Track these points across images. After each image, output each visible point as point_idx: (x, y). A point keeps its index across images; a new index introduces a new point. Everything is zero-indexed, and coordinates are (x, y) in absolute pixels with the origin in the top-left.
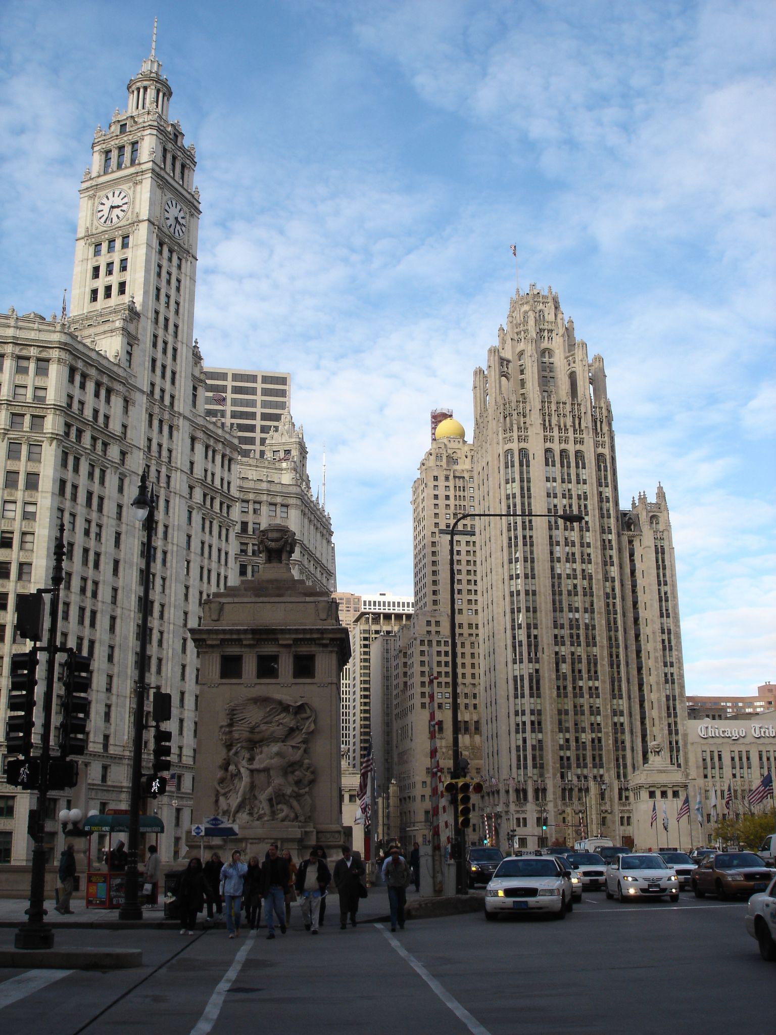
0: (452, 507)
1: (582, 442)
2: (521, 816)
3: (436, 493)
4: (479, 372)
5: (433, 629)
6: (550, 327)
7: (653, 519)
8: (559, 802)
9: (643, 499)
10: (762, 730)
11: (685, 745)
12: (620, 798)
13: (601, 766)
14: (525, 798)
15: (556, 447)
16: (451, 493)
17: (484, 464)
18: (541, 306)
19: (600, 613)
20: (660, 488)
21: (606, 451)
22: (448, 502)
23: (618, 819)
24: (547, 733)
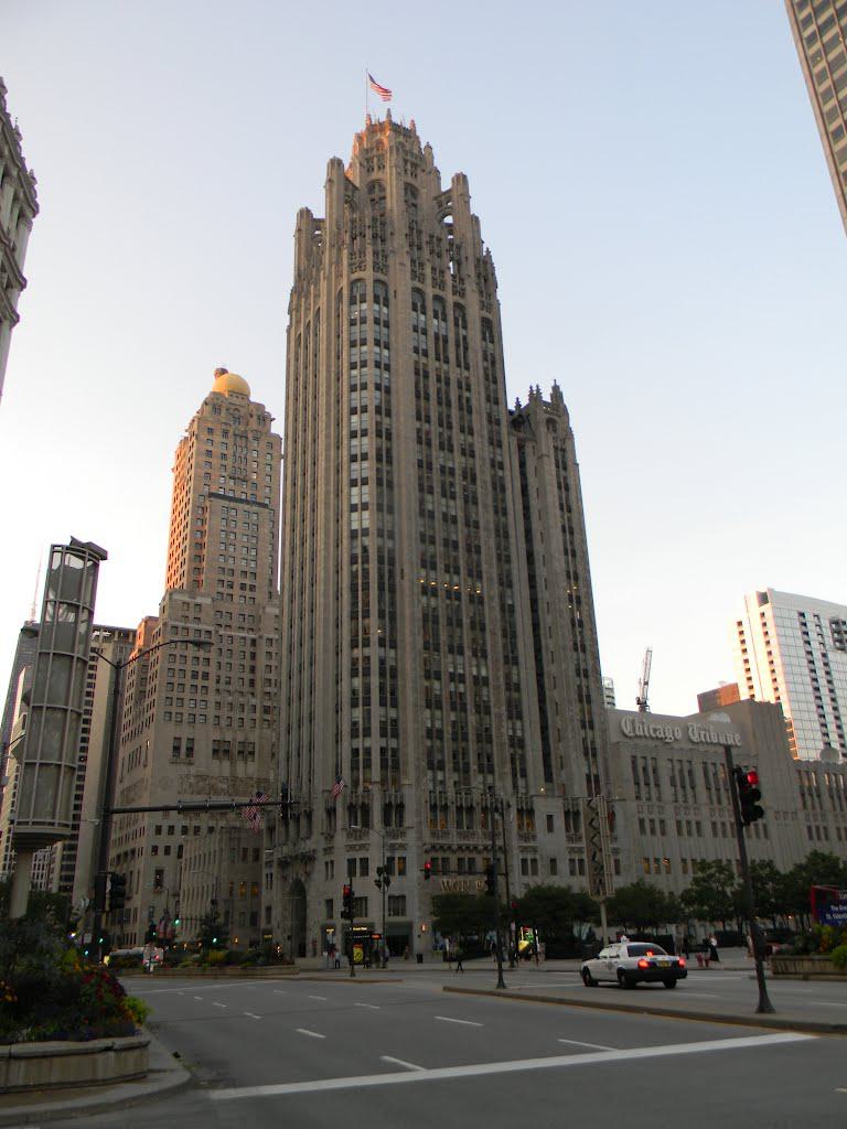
0: (229, 469)
1: (462, 294)
2: (358, 855)
3: (210, 448)
4: (305, 214)
5: (191, 614)
7: (551, 423)
8: (426, 832)
9: (535, 396)
10: (702, 733)
11: (605, 743)
12: (520, 827)
14: (367, 824)
16: (230, 453)
17: (311, 317)
19: (487, 529)
20: (556, 389)
22: (224, 462)
23: (516, 864)
24: (405, 708)
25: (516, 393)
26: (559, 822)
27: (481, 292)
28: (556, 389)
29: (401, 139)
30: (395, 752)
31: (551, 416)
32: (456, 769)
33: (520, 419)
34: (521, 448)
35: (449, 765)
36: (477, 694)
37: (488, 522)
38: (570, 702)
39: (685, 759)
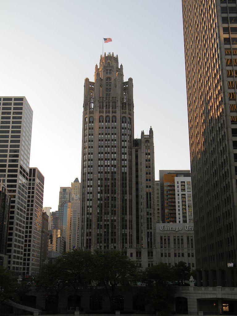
1: (115, 112)
6: (110, 68)
11: (155, 233)
13: (115, 242)
15: (104, 115)
18: (109, 61)
20: (151, 129)
21: (127, 115)
25: (137, 136)
26: (134, 255)
27: (123, 109)
28: (151, 129)
29: (109, 61)
30: (90, 240)
31: (148, 139)
32: (105, 243)
33: (137, 143)
34: (137, 151)
35: (103, 242)
36: (112, 224)
37: (118, 178)
38: (144, 223)
39: (180, 236)
